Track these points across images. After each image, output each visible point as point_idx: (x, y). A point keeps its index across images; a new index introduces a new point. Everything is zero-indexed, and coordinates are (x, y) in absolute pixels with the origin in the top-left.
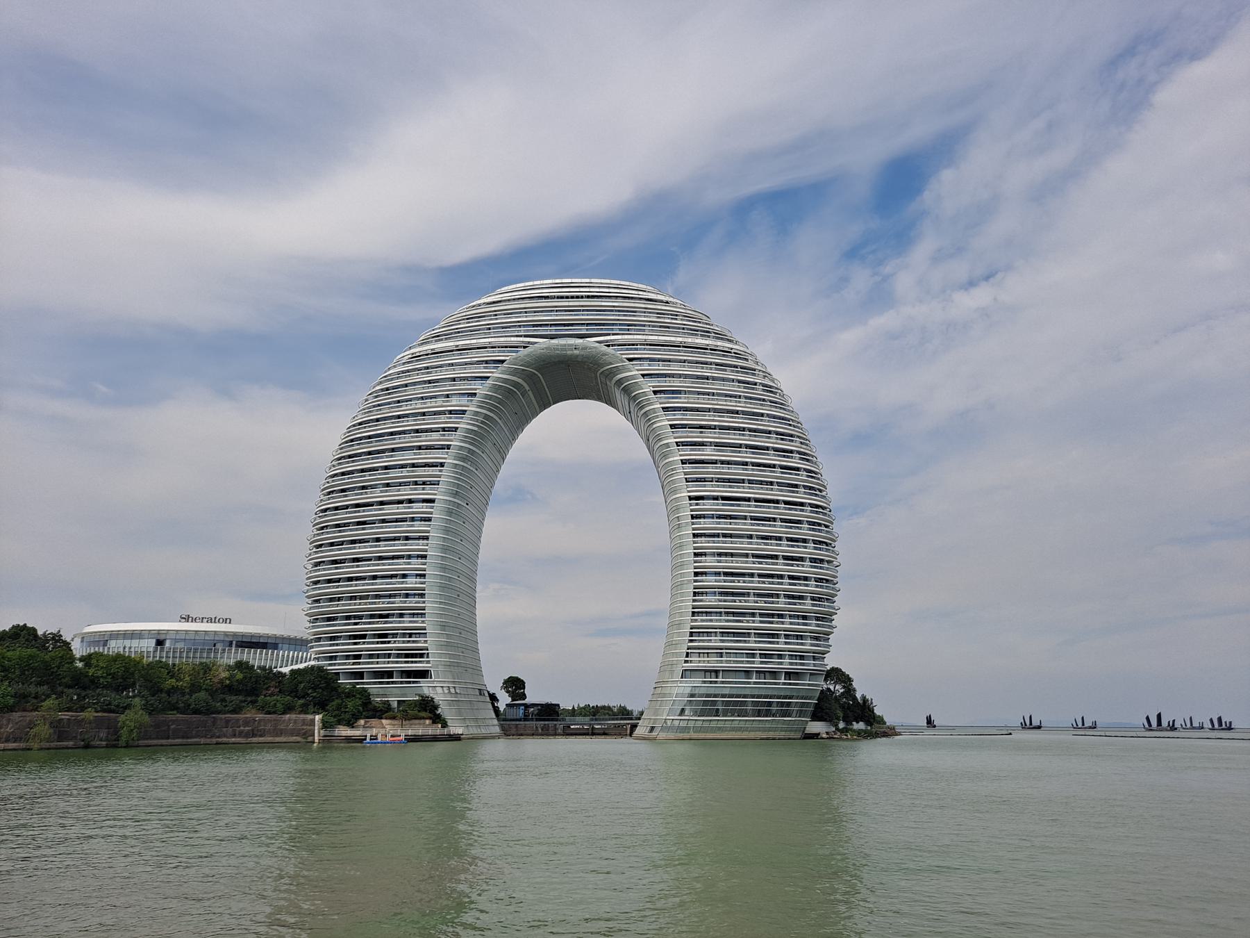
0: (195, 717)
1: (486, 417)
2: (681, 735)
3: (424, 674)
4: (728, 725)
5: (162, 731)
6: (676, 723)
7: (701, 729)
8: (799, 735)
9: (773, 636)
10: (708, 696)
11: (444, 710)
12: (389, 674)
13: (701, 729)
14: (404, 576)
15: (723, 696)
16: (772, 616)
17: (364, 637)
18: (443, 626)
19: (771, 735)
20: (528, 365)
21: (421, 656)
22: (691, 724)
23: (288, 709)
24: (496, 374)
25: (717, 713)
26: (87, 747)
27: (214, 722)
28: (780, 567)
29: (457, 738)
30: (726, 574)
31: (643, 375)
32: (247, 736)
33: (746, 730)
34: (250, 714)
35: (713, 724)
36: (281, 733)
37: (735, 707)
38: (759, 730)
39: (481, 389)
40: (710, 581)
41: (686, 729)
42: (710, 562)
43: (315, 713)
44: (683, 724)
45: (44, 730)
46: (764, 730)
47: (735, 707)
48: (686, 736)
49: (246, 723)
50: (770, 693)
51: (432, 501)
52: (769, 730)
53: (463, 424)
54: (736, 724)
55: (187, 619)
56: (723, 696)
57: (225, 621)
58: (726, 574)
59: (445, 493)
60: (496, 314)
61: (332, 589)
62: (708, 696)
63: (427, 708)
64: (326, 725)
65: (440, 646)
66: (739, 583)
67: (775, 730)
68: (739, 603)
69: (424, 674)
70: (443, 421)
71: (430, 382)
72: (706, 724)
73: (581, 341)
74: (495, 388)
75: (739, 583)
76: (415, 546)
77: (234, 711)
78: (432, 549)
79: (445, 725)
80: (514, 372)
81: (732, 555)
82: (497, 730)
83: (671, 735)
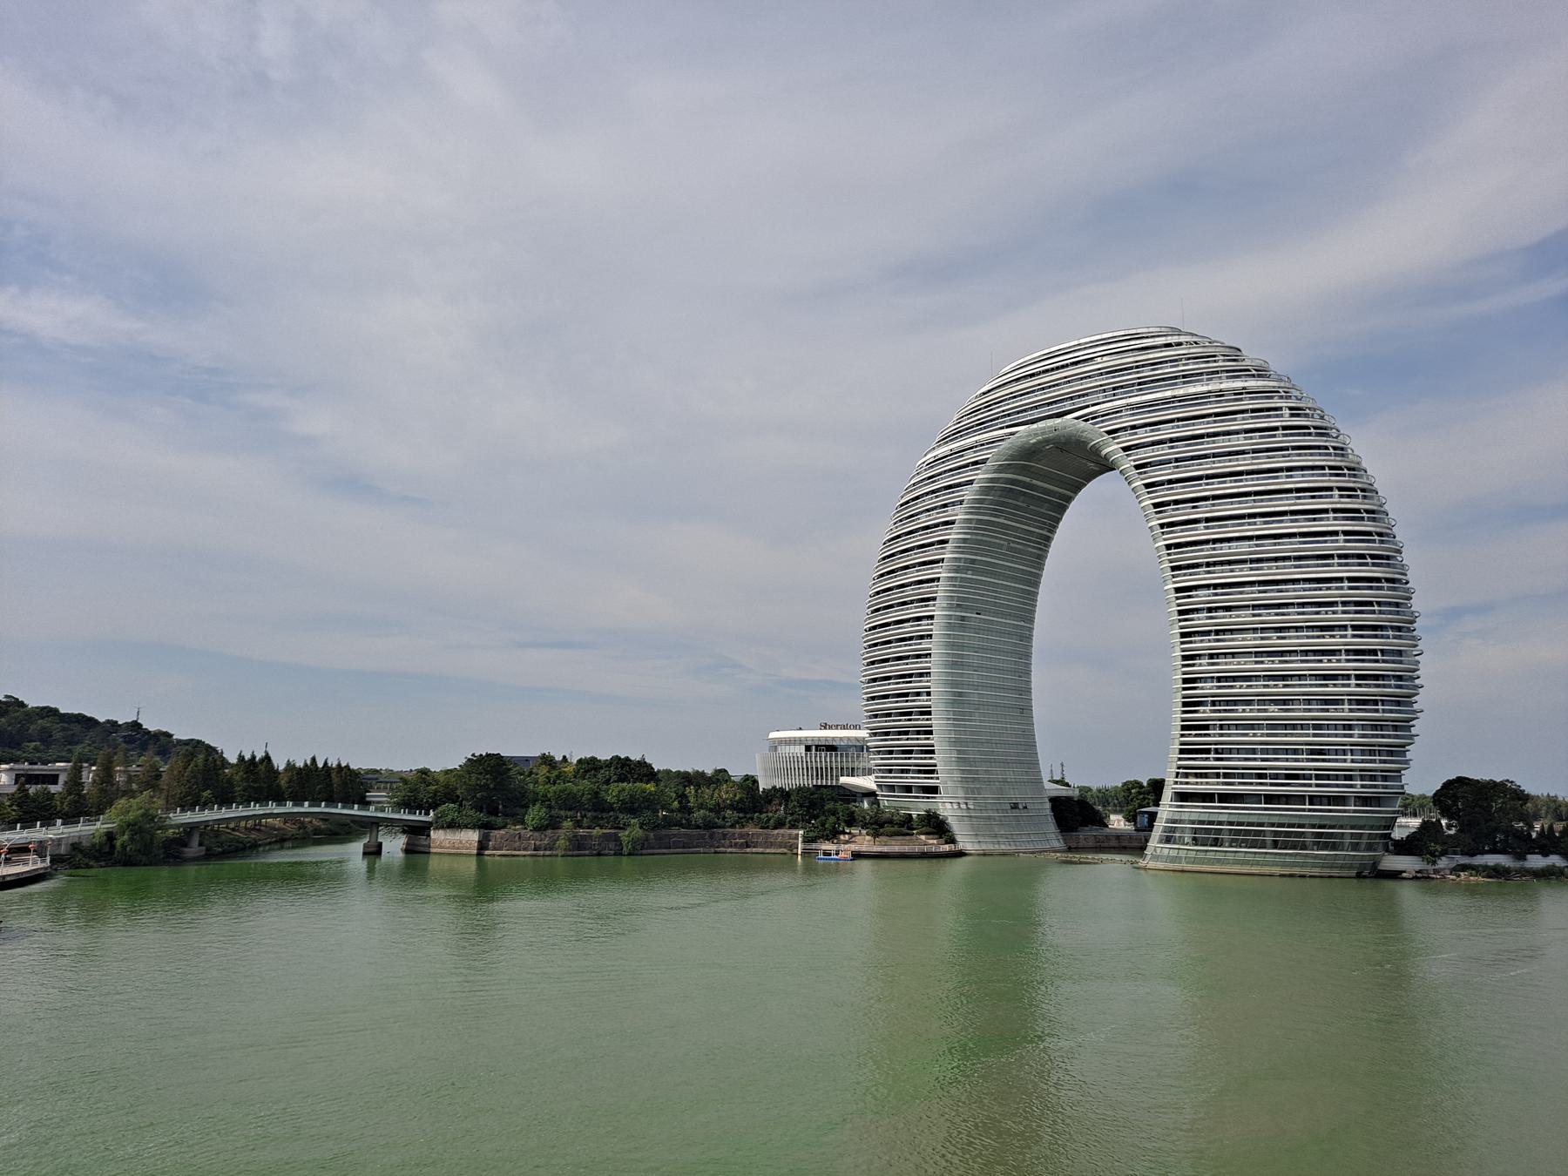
0: (695, 832)
2: (1171, 866)
4: (1230, 857)
5: (665, 844)
6: (1166, 852)
7: (1194, 861)
8: (1353, 873)
9: (1295, 752)
10: (1202, 822)
12: (908, 789)
14: (918, 694)
15: (1231, 823)
16: (1294, 727)
17: (911, 752)
18: (957, 742)
19: (1296, 871)
20: (1012, 457)
21: (932, 772)
22: (1183, 854)
23: (780, 824)
24: (981, 475)
25: (1216, 842)
26: (599, 854)
27: (711, 836)
28: (1295, 665)
29: (961, 854)
30: (1219, 679)
32: (741, 846)
34: (751, 830)
35: (1210, 856)
36: (772, 845)
38: (1275, 864)
39: (968, 494)
40: (1207, 688)
42: (1202, 666)
43: (793, 827)
44: (1173, 853)
45: (561, 842)
46: (1284, 865)
48: (1178, 866)
49: (741, 836)
50: (1286, 821)
51: (932, 617)
52: (1294, 865)
53: (953, 534)
54: (1240, 857)
55: (825, 726)
56: (1231, 823)
57: (855, 727)
58: (1219, 679)
59: (944, 609)
60: (988, 406)
61: (889, 704)
62: (1202, 822)
63: (936, 825)
64: (807, 840)
65: (947, 762)
66: (1240, 689)
67: (1302, 865)
68: (1242, 712)
69: (934, 790)
71: (933, 492)
72: (1201, 855)
73: (1058, 420)
74: (985, 491)
75: (1240, 689)
76: (921, 664)
77: (733, 826)
78: (935, 665)
79: (952, 841)
80: (1000, 469)
81: (1233, 655)
82: (1056, 841)
83: (1161, 865)
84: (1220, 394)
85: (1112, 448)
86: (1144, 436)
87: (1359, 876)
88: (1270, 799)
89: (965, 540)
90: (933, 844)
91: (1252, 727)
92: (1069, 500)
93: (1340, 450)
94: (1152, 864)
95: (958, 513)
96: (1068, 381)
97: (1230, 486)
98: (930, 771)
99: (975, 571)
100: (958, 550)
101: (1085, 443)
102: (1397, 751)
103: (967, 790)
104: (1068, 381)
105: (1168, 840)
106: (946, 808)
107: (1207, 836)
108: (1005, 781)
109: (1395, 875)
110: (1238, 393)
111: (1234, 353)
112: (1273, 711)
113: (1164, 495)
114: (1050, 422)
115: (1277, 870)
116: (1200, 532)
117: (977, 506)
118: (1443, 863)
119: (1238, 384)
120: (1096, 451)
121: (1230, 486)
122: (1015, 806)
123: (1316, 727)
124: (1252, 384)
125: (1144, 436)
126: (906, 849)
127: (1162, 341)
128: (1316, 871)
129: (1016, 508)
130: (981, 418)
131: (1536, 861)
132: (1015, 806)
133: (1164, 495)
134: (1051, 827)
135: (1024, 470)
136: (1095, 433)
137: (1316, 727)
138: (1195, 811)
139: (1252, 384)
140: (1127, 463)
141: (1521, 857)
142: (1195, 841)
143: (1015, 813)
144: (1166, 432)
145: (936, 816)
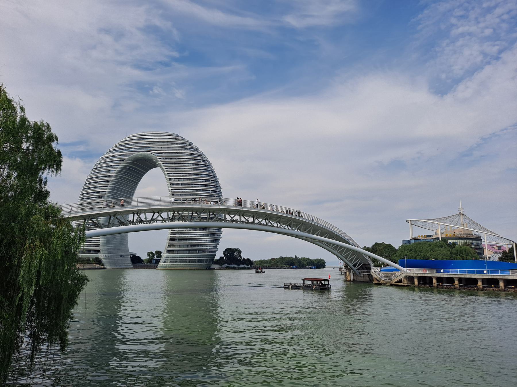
1: (120, 177)
3: (99, 251)
7: (170, 267)
11: (104, 261)
12: (90, 251)
13: (170, 267)
19: (193, 268)
24: (122, 164)
25: (176, 262)
31: (163, 163)
33: (185, 267)
37: (183, 260)
39: (117, 168)
41: (166, 267)
46: (191, 267)
47: (183, 260)
53: (112, 179)
63: (98, 261)
69: (99, 251)
70: (106, 179)
74: (122, 168)
79: (103, 265)
80: (128, 163)
82: (131, 266)
83: (162, 268)
84: (187, 153)
85: (160, 162)
86: (168, 161)
87: (206, 269)
88: (190, 251)
89: (115, 181)
90: (98, 266)
91: (187, 234)
92: (145, 173)
93: (212, 171)
94: (160, 268)
95: (114, 173)
96: (149, 143)
97: (187, 177)
98: (98, 246)
99: (117, 190)
100: (112, 184)
101: (152, 160)
102: (217, 241)
103: (108, 252)
104: (149, 143)
105: (165, 262)
106: (101, 256)
107: (174, 261)
108: (119, 250)
109: (214, 269)
110: (192, 154)
111: (191, 144)
112: (192, 231)
113: (171, 176)
114: (143, 153)
115: (189, 268)
116: (180, 187)
117: (120, 172)
118: (224, 266)
119: (191, 152)
120: (155, 162)
121: (187, 177)
122: (121, 256)
123: (201, 235)
124: (194, 152)
125: (168, 161)
126: (91, 267)
127: (174, 137)
128: (198, 268)
129: (131, 174)
130: (122, 147)
131: (241, 266)
132: (121, 256)
133: (171, 176)
134: (130, 262)
135: (134, 164)
136: (156, 158)
137: (201, 235)
138: (171, 255)
139: (194, 152)
140: (163, 167)
141: (239, 265)
142: (171, 262)
143: (122, 258)
144: (174, 161)
145: (99, 258)
